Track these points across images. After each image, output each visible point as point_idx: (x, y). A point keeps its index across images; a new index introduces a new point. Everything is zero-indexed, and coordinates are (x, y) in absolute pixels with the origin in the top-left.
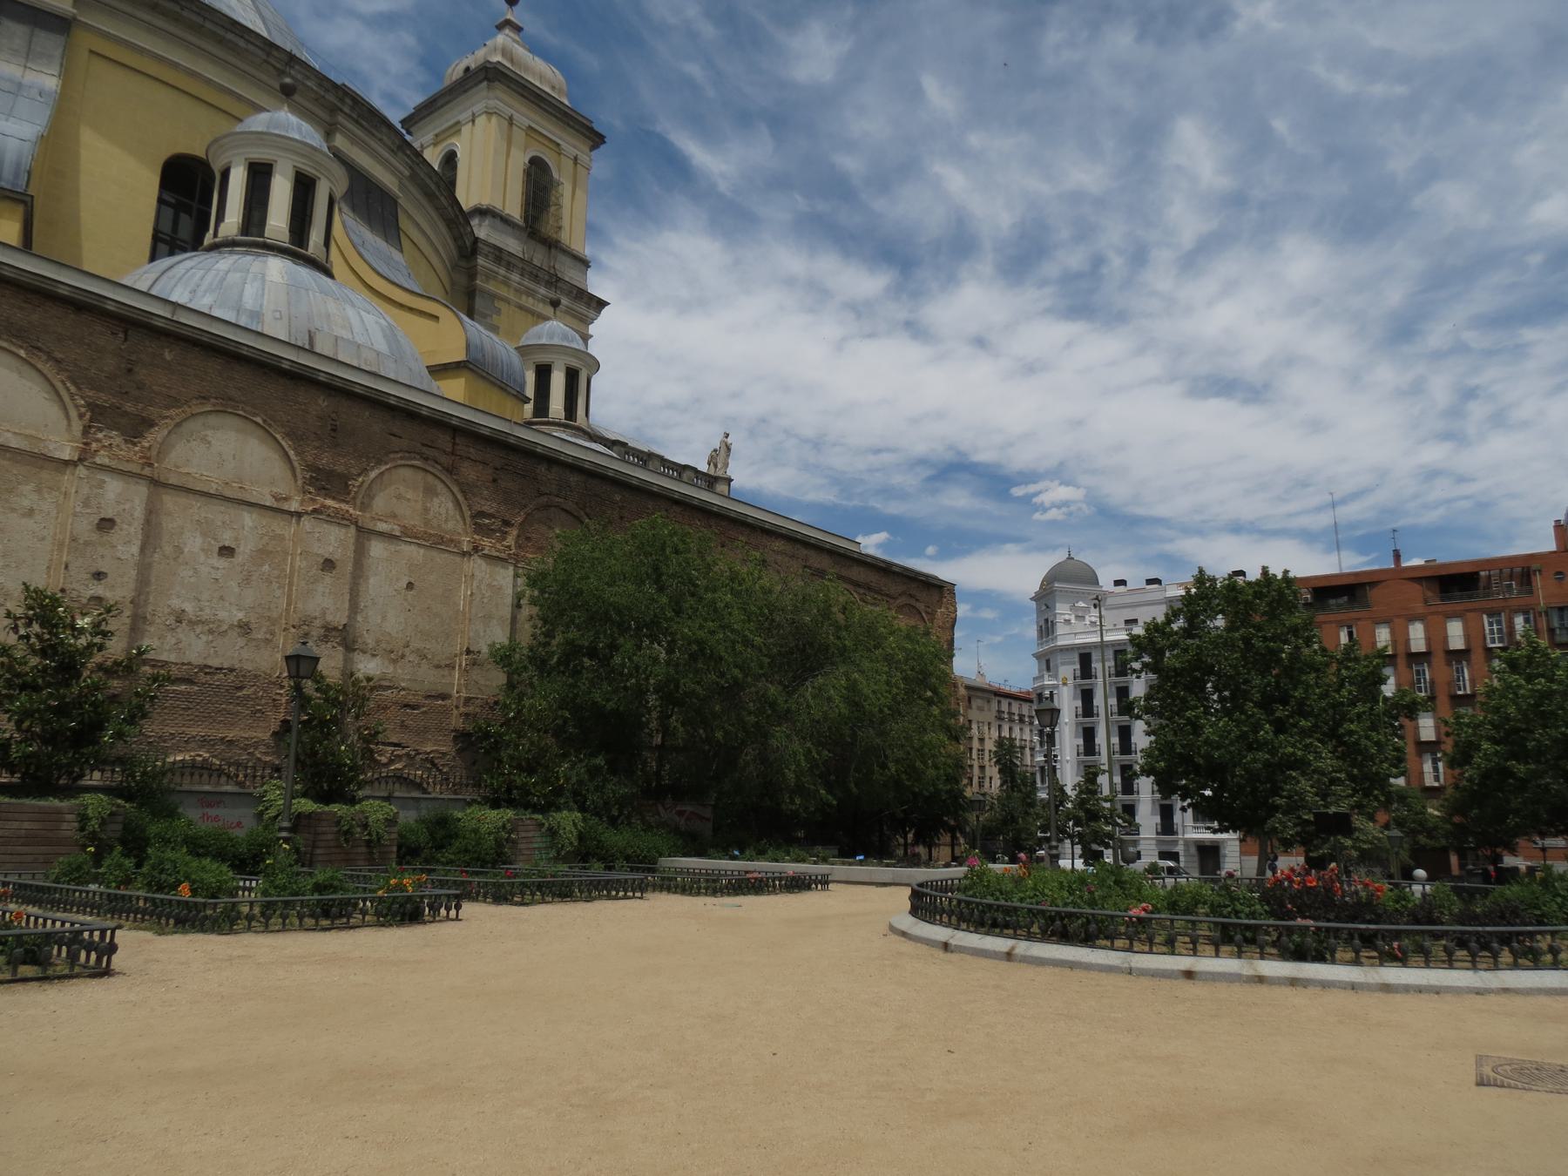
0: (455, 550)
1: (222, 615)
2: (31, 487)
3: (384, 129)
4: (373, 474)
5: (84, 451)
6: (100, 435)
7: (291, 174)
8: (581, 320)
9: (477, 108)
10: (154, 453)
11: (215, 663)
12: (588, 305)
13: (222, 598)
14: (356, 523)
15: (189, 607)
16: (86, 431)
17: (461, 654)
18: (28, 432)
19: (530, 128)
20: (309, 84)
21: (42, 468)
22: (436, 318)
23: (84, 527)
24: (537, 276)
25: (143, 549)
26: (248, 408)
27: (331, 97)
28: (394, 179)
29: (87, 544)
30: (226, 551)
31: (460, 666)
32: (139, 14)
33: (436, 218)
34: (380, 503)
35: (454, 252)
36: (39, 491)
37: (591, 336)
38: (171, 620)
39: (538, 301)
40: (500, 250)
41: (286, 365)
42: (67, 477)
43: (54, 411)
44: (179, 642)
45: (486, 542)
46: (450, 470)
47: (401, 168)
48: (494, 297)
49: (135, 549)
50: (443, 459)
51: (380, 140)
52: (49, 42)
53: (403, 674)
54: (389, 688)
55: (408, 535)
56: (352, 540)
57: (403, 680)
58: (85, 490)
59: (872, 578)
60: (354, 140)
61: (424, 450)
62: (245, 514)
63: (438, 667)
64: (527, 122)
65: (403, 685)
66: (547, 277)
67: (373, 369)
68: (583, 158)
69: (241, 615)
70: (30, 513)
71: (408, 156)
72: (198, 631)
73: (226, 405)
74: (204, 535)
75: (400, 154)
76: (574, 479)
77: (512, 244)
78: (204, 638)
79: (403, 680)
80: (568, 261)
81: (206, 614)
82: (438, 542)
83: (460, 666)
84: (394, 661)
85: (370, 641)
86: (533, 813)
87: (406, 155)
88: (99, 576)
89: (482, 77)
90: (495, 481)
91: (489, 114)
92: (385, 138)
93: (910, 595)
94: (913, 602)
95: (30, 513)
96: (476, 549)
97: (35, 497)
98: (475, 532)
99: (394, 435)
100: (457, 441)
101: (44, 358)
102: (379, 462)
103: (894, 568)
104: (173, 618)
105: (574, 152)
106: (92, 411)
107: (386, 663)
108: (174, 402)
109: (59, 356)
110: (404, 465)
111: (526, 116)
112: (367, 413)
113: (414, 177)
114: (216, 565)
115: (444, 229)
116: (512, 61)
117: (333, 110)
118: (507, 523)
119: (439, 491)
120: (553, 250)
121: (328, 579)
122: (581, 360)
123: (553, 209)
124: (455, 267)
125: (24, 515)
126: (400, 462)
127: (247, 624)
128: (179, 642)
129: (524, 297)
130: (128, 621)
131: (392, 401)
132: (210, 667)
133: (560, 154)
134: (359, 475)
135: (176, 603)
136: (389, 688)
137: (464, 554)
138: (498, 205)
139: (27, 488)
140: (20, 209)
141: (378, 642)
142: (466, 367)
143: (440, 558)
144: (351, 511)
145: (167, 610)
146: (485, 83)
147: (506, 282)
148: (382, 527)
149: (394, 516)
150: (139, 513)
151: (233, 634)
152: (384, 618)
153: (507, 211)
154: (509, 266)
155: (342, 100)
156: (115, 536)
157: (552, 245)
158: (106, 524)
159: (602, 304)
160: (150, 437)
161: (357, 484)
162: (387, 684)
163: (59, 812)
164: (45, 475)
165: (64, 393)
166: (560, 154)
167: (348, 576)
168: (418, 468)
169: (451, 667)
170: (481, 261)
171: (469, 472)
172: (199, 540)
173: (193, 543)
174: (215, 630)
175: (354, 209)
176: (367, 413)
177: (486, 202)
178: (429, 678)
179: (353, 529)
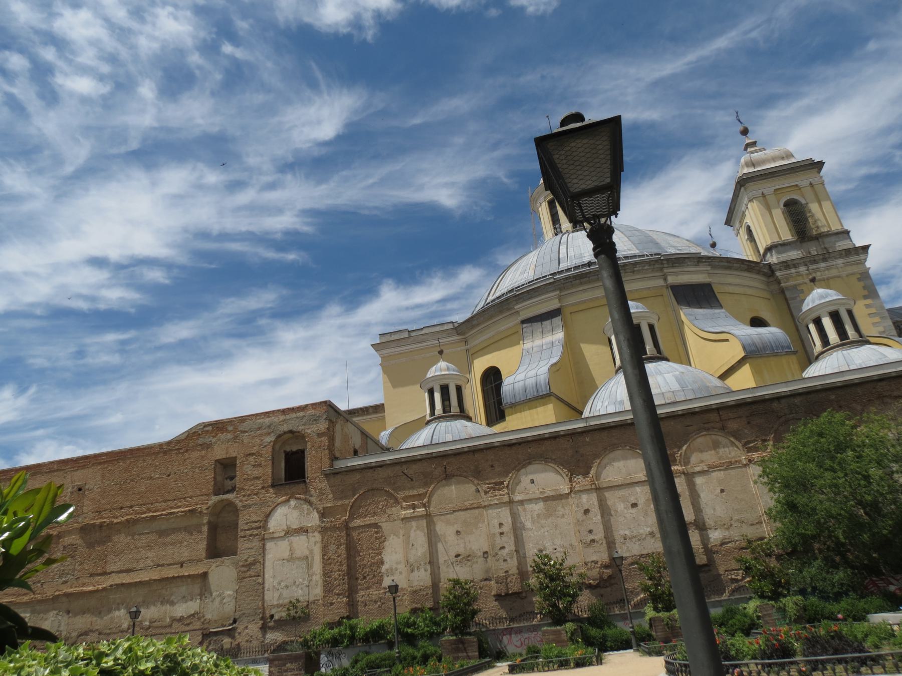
0: (740, 465)
1: (641, 531)
2: (560, 507)
3: (687, 260)
4: (684, 448)
5: (571, 488)
6: (575, 479)
8: (858, 264)
9: (746, 200)
10: (595, 478)
11: (645, 552)
12: (858, 254)
13: (639, 525)
14: (684, 473)
15: (627, 532)
16: (570, 480)
17: (763, 515)
18: (555, 488)
19: (776, 190)
20: (645, 268)
21: (562, 499)
22: (727, 340)
23: (580, 515)
24: (815, 260)
25: (602, 516)
26: (623, 445)
27: (657, 266)
28: (704, 275)
29: (583, 521)
30: (634, 505)
31: (765, 521)
32: (578, 289)
34: (694, 459)
35: (764, 279)
36: (563, 507)
37: (869, 268)
38: (622, 540)
39: (824, 271)
40: (785, 262)
42: (570, 501)
43: (559, 478)
44: (628, 547)
45: (755, 455)
46: (723, 428)
48: (795, 286)
49: (599, 517)
51: (688, 265)
52: (557, 320)
53: (735, 533)
54: (730, 542)
55: (712, 468)
56: (684, 481)
57: (736, 536)
58: (576, 502)
60: (676, 274)
61: (706, 425)
62: (637, 488)
63: (752, 525)
65: (736, 539)
67: (673, 400)
68: (814, 181)
69: (649, 529)
70: (563, 516)
71: (705, 262)
72: (634, 541)
73: (613, 447)
74: (623, 502)
75: (701, 264)
76: (797, 400)
77: (794, 254)
78: (637, 543)
79: (736, 536)
80: (833, 239)
81: (635, 533)
82: (729, 465)
83: (765, 521)
84: (728, 529)
85: (711, 523)
86: (769, 601)
87: (703, 262)
88: (590, 532)
89: (739, 187)
90: (749, 423)
91: (751, 201)
92: (689, 263)
95: (563, 516)
96: (750, 461)
97: (563, 510)
98: (748, 452)
99: (688, 426)
100: (721, 413)
101: (550, 460)
102: (685, 443)
104: (623, 539)
105: (807, 183)
106: (570, 472)
107: (723, 530)
108: (596, 456)
109: (554, 457)
110: (698, 437)
111: (769, 187)
112: (672, 423)
113: (714, 267)
114: (632, 512)
116: (754, 165)
117: (661, 269)
118: (764, 441)
119: (720, 440)
120: (820, 240)
123: (810, 220)
124: (768, 284)
125: (561, 518)
126: (695, 437)
127: (653, 532)
128: (628, 547)
130: (606, 545)
131: (680, 413)
132: (644, 555)
133: (800, 189)
134: (679, 451)
135: (621, 532)
136: (730, 542)
137: (745, 465)
138: (776, 240)
139: (559, 508)
140: (552, 398)
141: (715, 522)
142: (746, 358)
143: (732, 472)
144: (680, 468)
145: (619, 537)
146: (742, 189)
147: (799, 274)
148: (697, 469)
149: (702, 462)
150: (596, 503)
151: (648, 538)
152: (714, 510)
154: (795, 266)
155: (662, 264)
156: (591, 514)
157: (819, 237)
158: (587, 511)
159: (865, 248)
160: (591, 472)
161: (679, 455)
162: (728, 540)
163: (559, 631)
164: (563, 501)
165: (559, 470)
166: (800, 189)
167: (688, 497)
168: (706, 435)
169: (760, 523)
170: (778, 274)
171: (733, 425)
172: (622, 505)
173: (621, 507)
174: (640, 539)
175: (689, 304)
176: (672, 423)
177: (769, 242)
178: (751, 532)
179: (683, 476)
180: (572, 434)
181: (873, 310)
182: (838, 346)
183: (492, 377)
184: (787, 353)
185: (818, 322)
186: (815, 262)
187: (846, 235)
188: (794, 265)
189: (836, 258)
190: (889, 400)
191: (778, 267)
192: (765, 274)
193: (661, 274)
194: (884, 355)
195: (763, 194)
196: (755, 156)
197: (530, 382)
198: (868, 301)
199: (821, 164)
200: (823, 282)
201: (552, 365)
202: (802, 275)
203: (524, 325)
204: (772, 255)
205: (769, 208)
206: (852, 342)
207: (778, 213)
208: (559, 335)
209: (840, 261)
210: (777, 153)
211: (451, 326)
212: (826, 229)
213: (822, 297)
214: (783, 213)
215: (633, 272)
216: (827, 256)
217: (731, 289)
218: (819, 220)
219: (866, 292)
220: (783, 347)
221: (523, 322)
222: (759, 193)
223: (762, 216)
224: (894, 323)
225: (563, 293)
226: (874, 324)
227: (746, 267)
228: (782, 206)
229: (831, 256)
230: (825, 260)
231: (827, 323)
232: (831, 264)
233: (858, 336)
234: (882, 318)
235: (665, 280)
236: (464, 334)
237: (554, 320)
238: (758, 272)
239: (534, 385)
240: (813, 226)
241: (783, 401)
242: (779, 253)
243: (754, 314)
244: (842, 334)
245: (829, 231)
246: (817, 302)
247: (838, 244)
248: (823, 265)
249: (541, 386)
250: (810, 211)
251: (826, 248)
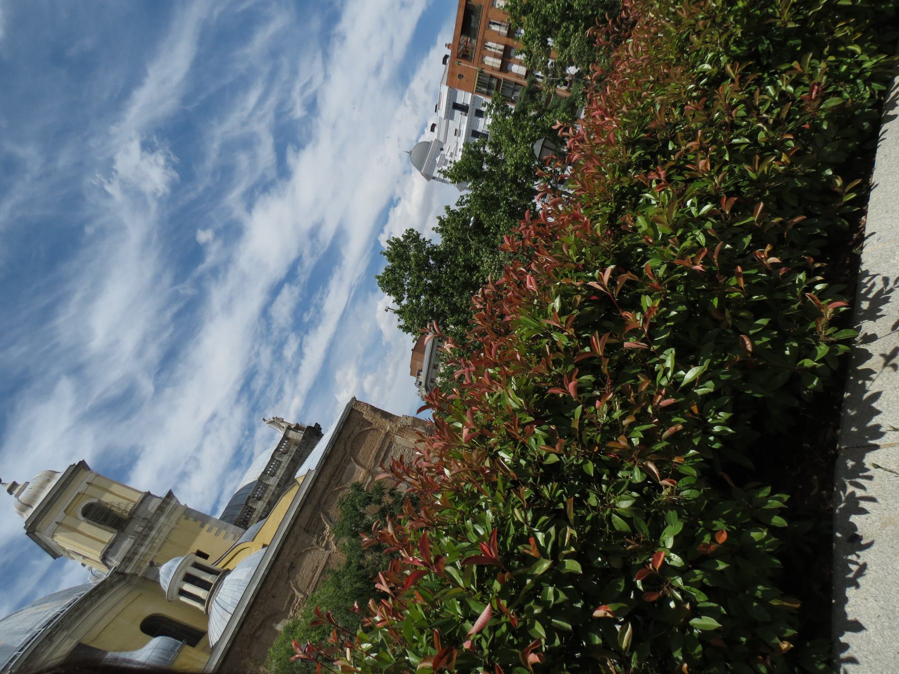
8: (175, 509)
12: (169, 503)
19: (65, 511)
24: (145, 536)
33: (96, 605)
40: (125, 558)
51: (43, 653)
59: (329, 470)
64: (62, 513)
66: (147, 529)
71: (57, 633)
75: (54, 639)
77: (127, 544)
80: (142, 508)
91: (53, 537)
92: (42, 650)
93: (349, 437)
94: (353, 437)
103: (328, 452)
111: (57, 514)
113: (68, 628)
115: (105, 597)
116: (29, 506)
122: (181, 571)
129: (155, 545)
133: (84, 494)
138: (103, 547)
146: (37, 533)
153: (107, 541)
154: (135, 553)
157: (133, 514)
170: (128, 571)
177: (99, 554)
181: (215, 529)
184: (179, 651)
185: (182, 593)
186: (146, 536)
187: (149, 497)
189: (157, 520)
190: (259, 633)
191: (123, 567)
192: (119, 581)
194: (237, 580)
195: (57, 523)
196: (22, 496)
198: (207, 526)
199: (82, 465)
202: (147, 554)
204: (111, 561)
205: (74, 530)
206: (216, 585)
207: (85, 527)
209: (162, 519)
210: (40, 480)
212: (129, 509)
213: (168, 574)
214: (88, 523)
216: (150, 525)
217: (102, 625)
218: (119, 504)
219: (199, 523)
220: (172, 650)
222: (54, 525)
223: (74, 539)
224: (235, 524)
226: (225, 537)
227: (97, 596)
228: (82, 518)
229: (153, 521)
230: (151, 529)
231: (188, 587)
233: (216, 576)
234: (225, 528)
238: (112, 586)
240: (120, 511)
242: (114, 555)
243: (139, 622)
244: (205, 585)
245: (135, 505)
246: (169, 581)
247: (149, 508)
248: (153, 533)
250: (107, 504)
251: (144, 519)
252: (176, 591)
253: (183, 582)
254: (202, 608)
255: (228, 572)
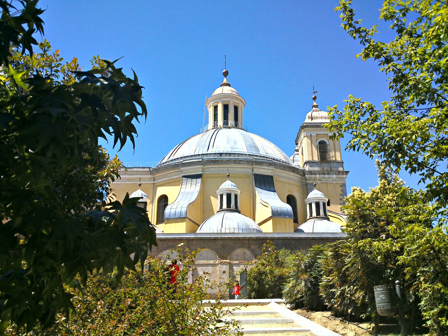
7: (226, 194)
8: (342, 179)
12: (343, 174)
24: (324, 173)
33: (288, 173)
35: (300, 177)
41: (212, 238)
47: (272, 169)
50: (247, 246)
52: (199, 180)
66: (327, 172)
75: (270, 166)
76: (280, 241)
90: (259, 247)
115: (292, 174)
121: (224, 274)
138: (311, 159)
140: (187, 219)
144: (228, 261)
154: (315, 174)
157: (331, 162)
170: (306, 176)
171: (253, 247)
180: (188, 240)
182: (315, 218)
183: (164, 200)
185: (310, 205)
186: (324, 174)
188: (315, 173)
189: (333, 174)
191: (307, 173)
192: (301, 175)
193: (251, 167)
197: (178, 210)
200: (325, 184)
201: (190, 203)
203: (184, 178)
208: (198, 188)
211: (148, 170)
215: (239, 164)
217: (282, 180)
219: (342, 193)
221: (183, 177)
225: (204, 167)
228: (318, 143)
230: (328, 174)
231: (314, 206)
232: (331, 176)
235: (253, 170)
236: (154, 175)
237: (198, 179)
238: (298, 173)
239: (180, 212)
241: (275, 241)
244: (318, 213)
248: (327, 176)
249: (182, 212)
252: (310, 202)
253: (315, 203)
254: (308, 217)
255: (328, 219)
